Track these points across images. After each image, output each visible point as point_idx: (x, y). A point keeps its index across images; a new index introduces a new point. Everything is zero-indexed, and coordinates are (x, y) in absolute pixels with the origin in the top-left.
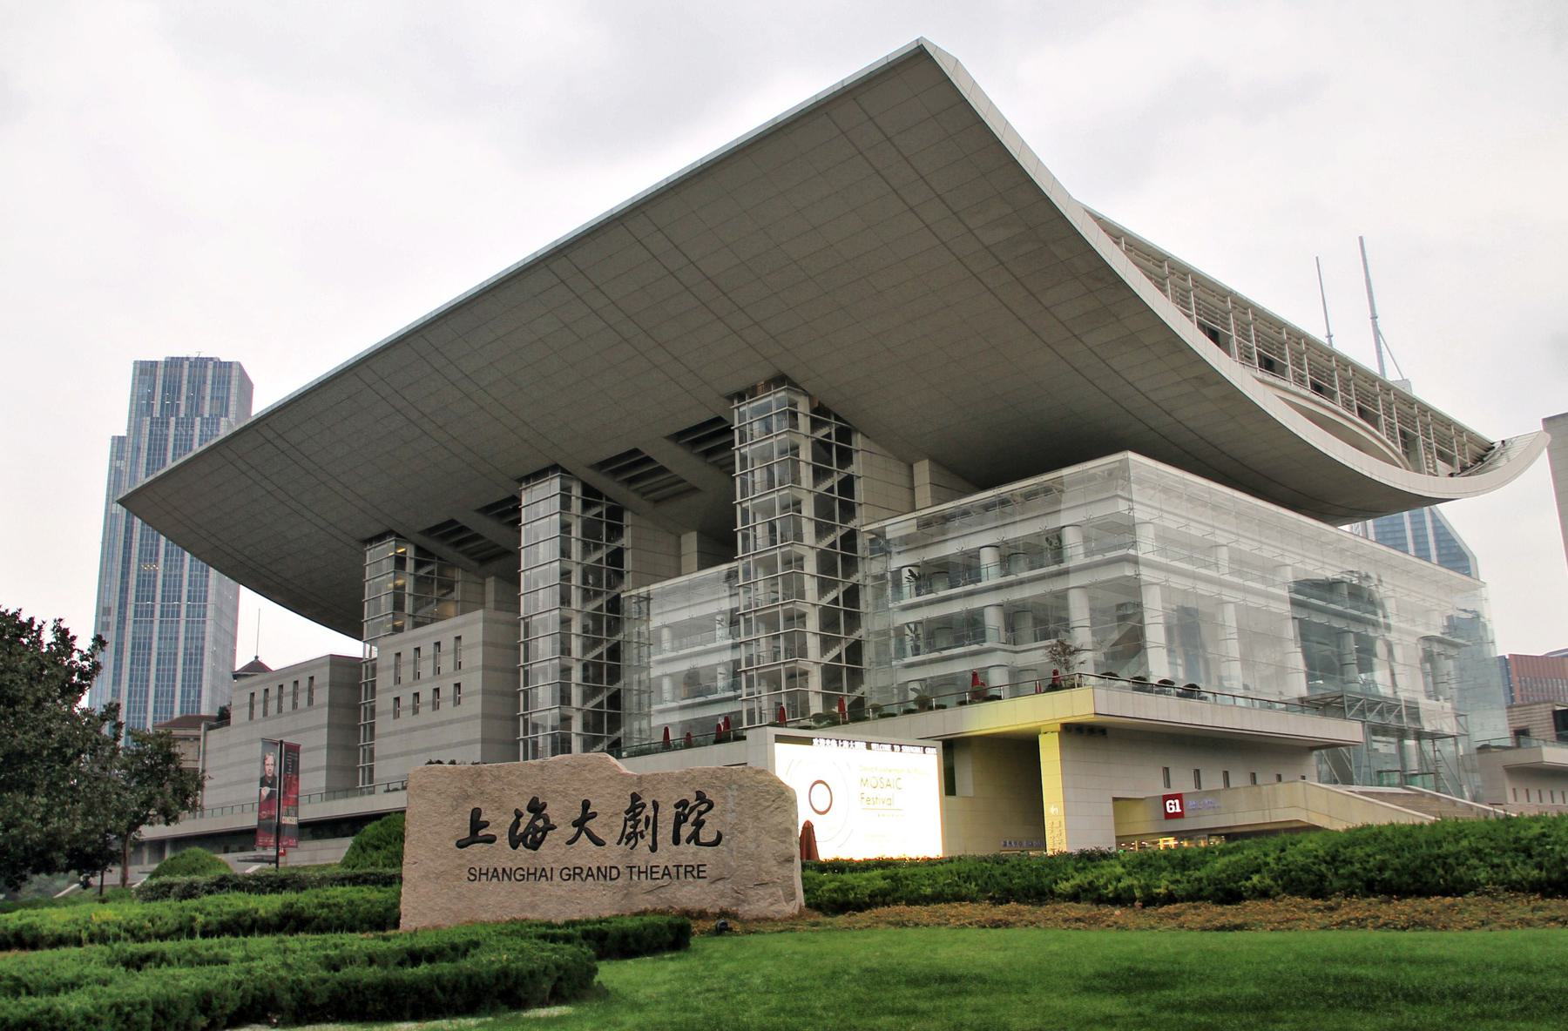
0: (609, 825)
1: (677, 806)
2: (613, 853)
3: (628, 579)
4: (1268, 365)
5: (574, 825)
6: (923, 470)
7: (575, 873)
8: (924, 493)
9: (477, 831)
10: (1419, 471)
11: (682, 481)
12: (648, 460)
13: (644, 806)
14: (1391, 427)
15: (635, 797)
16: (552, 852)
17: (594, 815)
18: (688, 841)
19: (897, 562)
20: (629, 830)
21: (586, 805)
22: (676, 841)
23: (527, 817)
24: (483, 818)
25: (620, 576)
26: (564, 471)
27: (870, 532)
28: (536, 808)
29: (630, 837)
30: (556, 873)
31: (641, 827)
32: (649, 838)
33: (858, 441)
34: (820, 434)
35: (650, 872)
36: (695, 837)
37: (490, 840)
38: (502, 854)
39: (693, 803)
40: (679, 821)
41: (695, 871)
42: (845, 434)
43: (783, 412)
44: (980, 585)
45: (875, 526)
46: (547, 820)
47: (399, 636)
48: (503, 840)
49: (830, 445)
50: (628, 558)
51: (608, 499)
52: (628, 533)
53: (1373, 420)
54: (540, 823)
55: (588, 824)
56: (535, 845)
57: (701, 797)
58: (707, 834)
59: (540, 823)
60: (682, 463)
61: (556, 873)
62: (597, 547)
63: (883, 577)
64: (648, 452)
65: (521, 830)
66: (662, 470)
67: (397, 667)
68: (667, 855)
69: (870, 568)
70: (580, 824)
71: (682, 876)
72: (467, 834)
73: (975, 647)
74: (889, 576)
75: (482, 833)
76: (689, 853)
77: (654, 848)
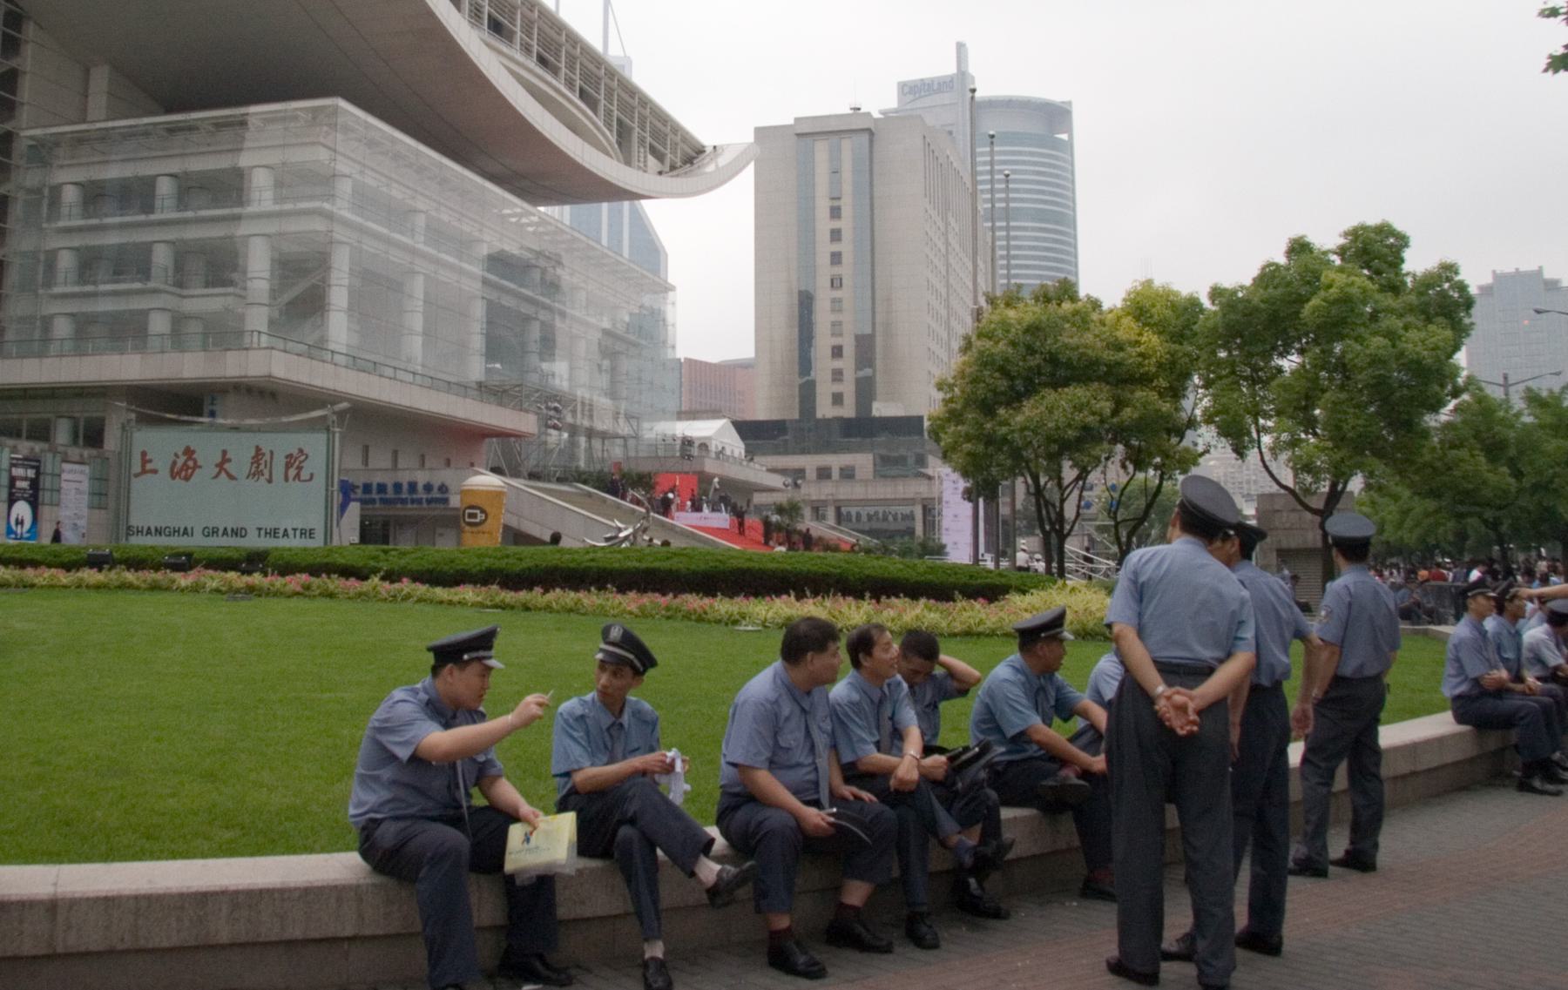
4: (496, 27)
6: (100, 79)
8: (98, 101)
10: (628, 163)
14: (609, 113)
15: (258, 449)
21: (224, 453)
22: (286, 479)
27: (32, 138)
33: (30, 30)
36: (298, 476)
37: (155, 472)
40: (288, 466)
44: (152, 217)
45: (38, 132)
48: (164, 472)
53: (592, 104)
55: (226, 466)
56: (187, 479)
57: (301, 451)
63: (38, 191)
70: (220, 466)
73: (137, 285)
74: (46, 192)
75: (149, 466)
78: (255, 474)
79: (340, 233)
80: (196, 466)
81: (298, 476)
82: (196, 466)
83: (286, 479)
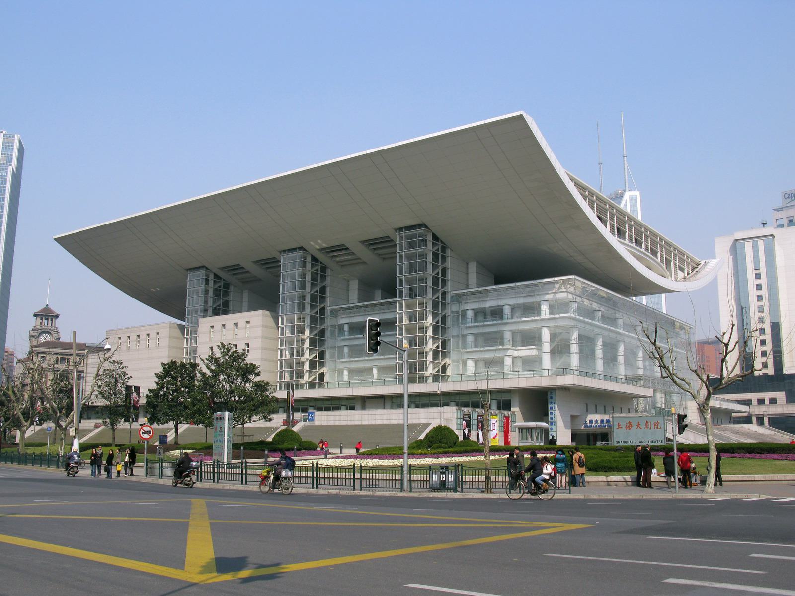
6: (473, 267)
11: (360, 259)
21: (639, 422)
33: (449, 252)
42: (444, 249)
50: (328, 289)
51: (321, 263)
70: (638, 426)
78: (647, 427)
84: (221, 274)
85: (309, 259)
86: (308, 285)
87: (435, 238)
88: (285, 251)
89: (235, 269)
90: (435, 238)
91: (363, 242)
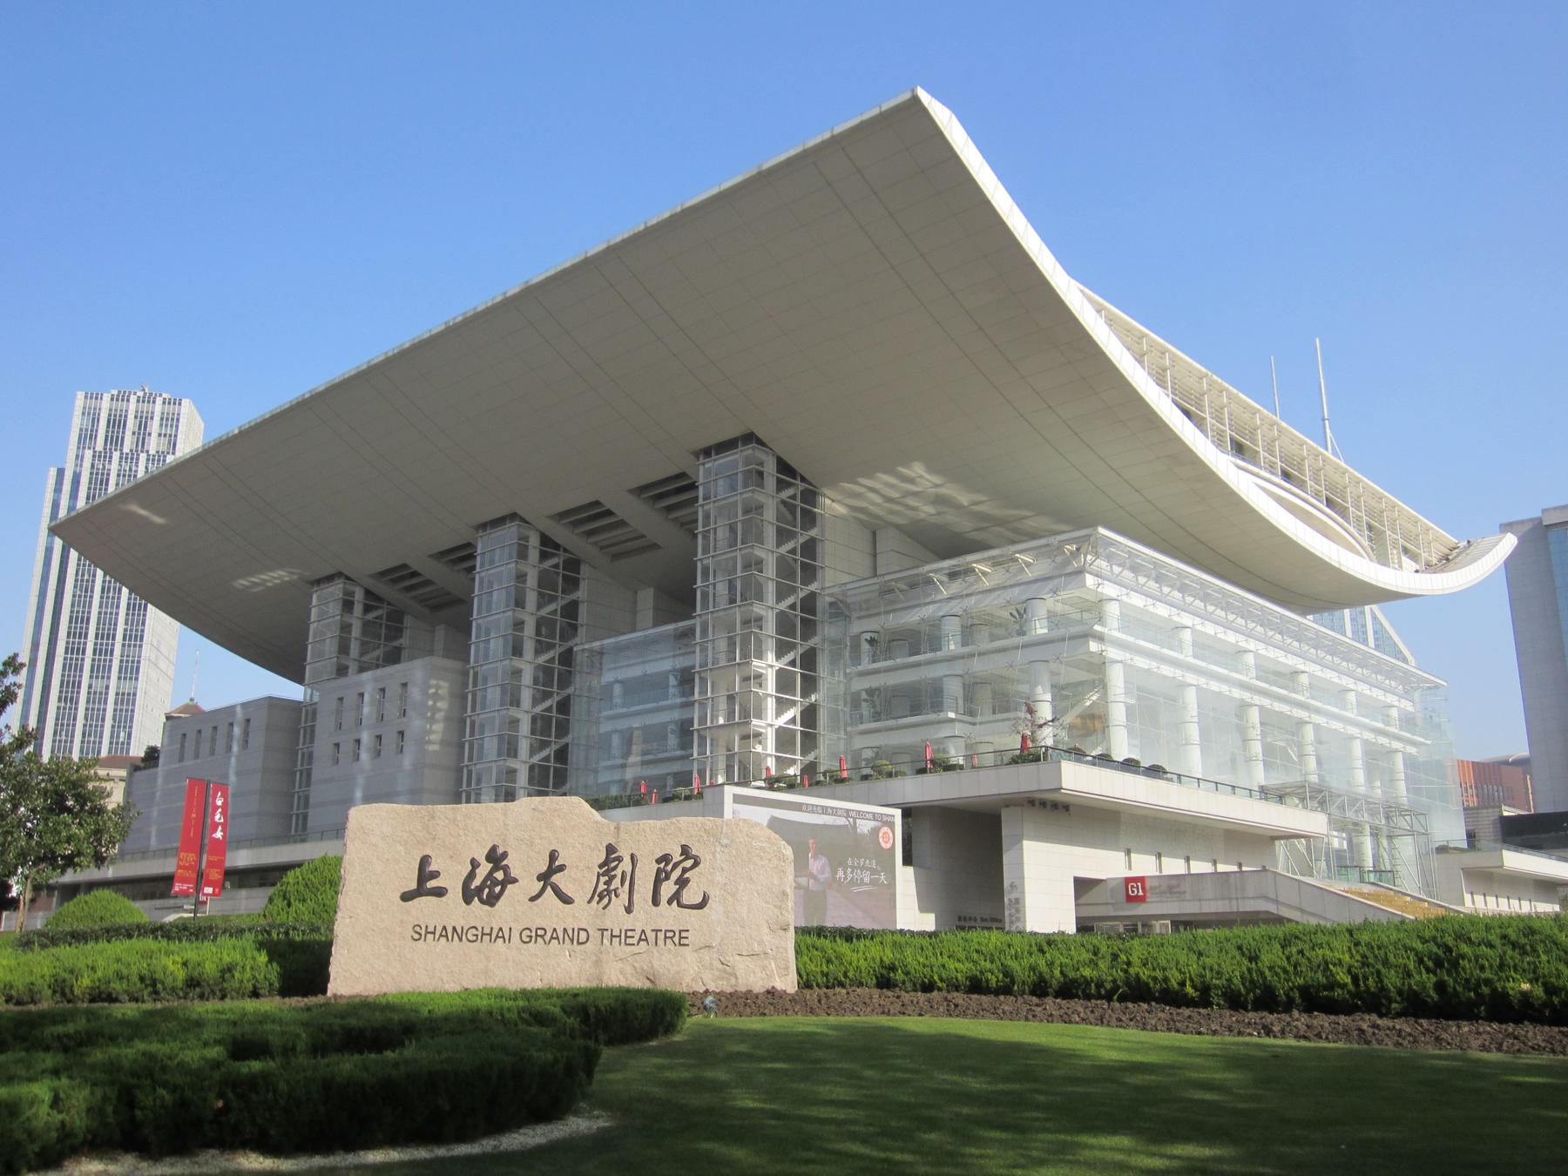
0: (579, 879)
1: (658, 861)
2: (582, 914)
3: (582, 631)
4: (1239, 449)
5: (539, 879)
7: (536, 935)
9: (425, 884)
11: (643, 536)
12: (609, 513)
13: (619, 859)
15: (610, 849)
16: (513, 908)
17: (561, 868)
18: (670, 902)
19: (856, 628)
20: (602, 887)
21: (553, 856)
22: (656, 901)
23: (485, 868)
24: (433, 867)
25: (575, 628)
26: (523, 520)
28: (496, 858)
29: (602, 895)
30: (516, 935)
31: (616, 883)
32: (624, 896)
34: (785, 494)
35: (625, 936)
37: (440, 892)
38: (452, 910)
39: (677, 857)
41: (679, 938)
43: (750, 471)
46: (506, 869)
47: (342, 681)
48: (456, 892)
49: (795, 506)
51: (565, 550)
52: (583, 585)
53: (1343, 513)
54: (499, 875)
55: (555, 878)
56: (492, 901)
57: (685, 851)
58: (691, 895)
59: (499, 875)
60: (642, 517)
61: (516, 935)
62: (553, 599)
64: (608, 504)
65: (477, 882)
66: (622, 523)
67: (339, 712)
68: (645, 916)
69: (828, 630)
70: (545, 877)
71: (661, 942)
72: (413, 885)
75: (431, 884)
76: (670, 916)
77: (629, 910)
79: (1112, 653)
80: (510, 880)
81: (676, 898)
82: (510, 880)
83: (656, 901)
84: (381, 588)
85: (534, 541)
86: (531, 599)
87: (784, 467)
88: (484, 526)
89: (401, 575)
90: (784, 467)
91: (631, 491)
